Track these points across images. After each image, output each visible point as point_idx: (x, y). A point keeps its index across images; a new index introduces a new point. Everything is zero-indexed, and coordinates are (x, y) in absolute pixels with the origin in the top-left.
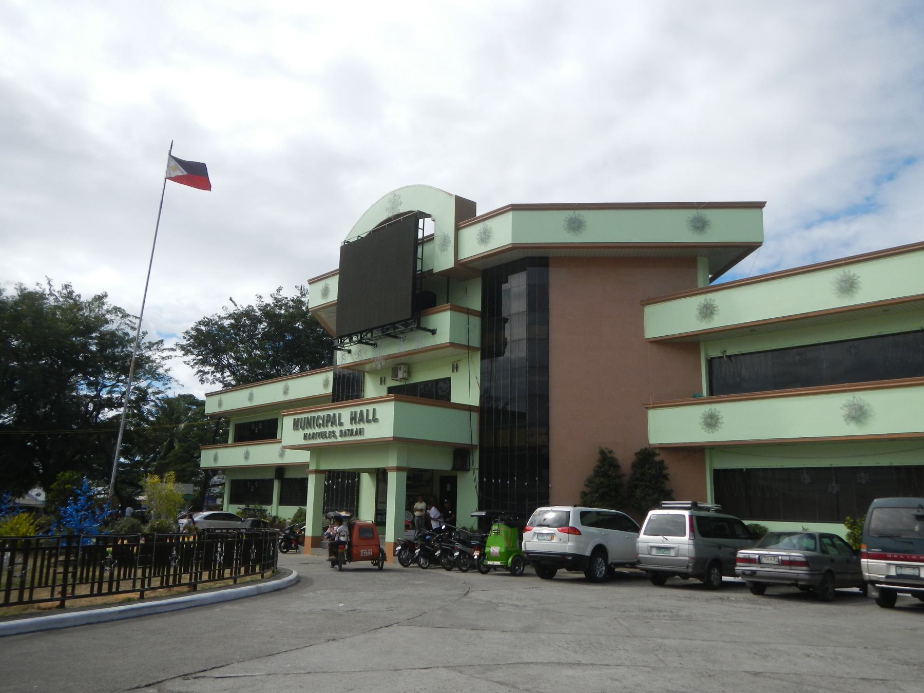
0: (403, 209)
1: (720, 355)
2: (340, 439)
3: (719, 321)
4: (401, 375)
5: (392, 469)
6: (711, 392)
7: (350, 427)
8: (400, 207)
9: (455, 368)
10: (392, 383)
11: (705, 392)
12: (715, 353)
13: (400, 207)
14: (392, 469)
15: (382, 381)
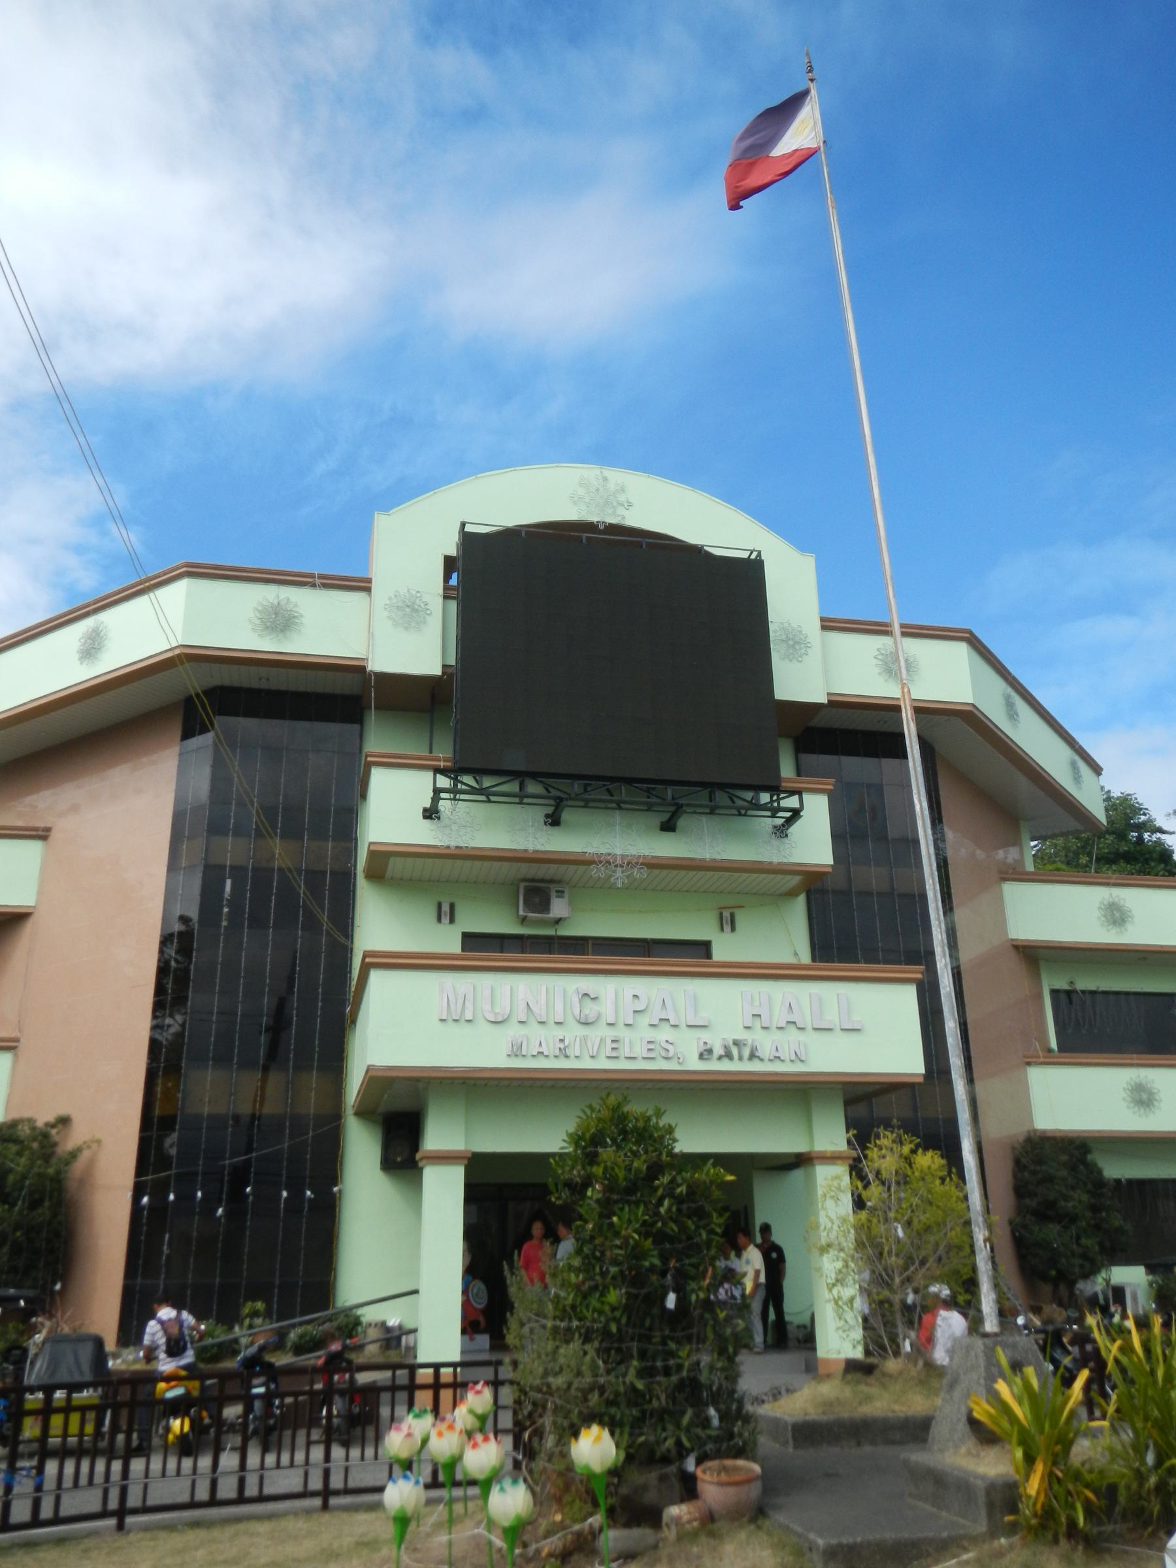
0: (634, 520)
1: (1066, 987)
2: (694, 1064)
3: (1137, 935)
4: (558, 908)
5: (832, 1158)
6: (1063, 1048)
7: (741, 1035)
8: (621, 511)
9: (727, 921)
10: (495, 921)
11: (1054, 1044)
12: (1063, 985)
13: (621, 511)
14: (832, 1158)
15: (446, 914)
